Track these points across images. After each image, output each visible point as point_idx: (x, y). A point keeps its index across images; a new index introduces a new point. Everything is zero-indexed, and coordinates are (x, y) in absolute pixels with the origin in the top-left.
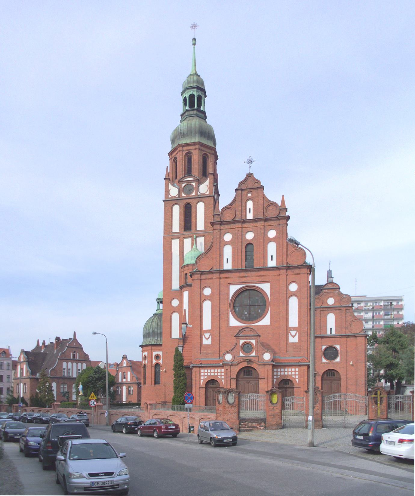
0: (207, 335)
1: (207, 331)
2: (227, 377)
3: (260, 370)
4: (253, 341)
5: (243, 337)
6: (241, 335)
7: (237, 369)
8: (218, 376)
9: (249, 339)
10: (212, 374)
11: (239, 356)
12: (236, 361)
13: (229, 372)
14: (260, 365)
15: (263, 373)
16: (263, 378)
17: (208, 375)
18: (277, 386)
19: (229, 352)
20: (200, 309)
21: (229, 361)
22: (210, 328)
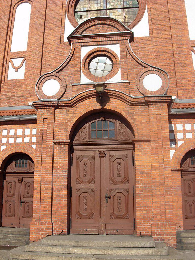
0: (17, 62)
1: (17, 55)
2: (45, 138)
3: (136, 117)
4: (116, 49)
5: (89, 40)
6: (85, 34)
7: (72, 117)
8: (31, 143)
9: (103, 43)
10: (19, 140)
11: (79, 83)
12: (70, 96)
13: (51, 126)
14: (133, 104)
15: (143, 125)
16: (145, 138)
17: (10, 142)
18: (179, 168)
19: (53, 74)
20: (9, 16)
21: (52, 97)
22: (24, 48)
